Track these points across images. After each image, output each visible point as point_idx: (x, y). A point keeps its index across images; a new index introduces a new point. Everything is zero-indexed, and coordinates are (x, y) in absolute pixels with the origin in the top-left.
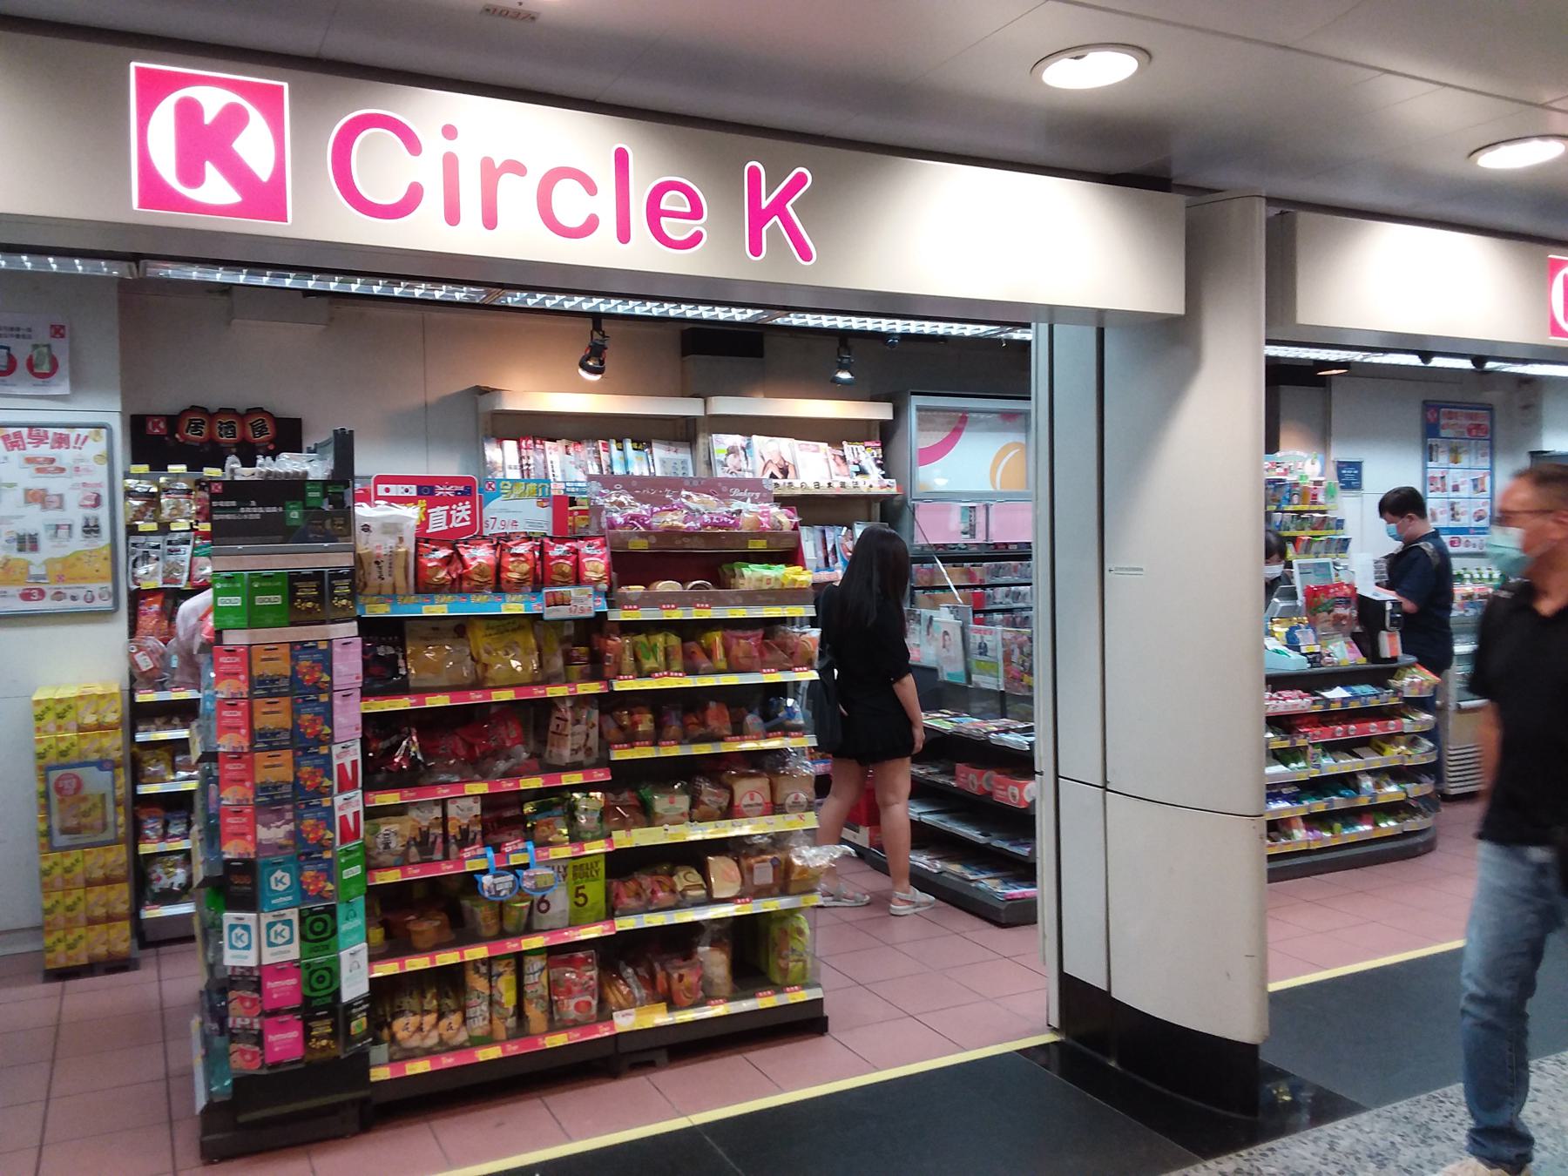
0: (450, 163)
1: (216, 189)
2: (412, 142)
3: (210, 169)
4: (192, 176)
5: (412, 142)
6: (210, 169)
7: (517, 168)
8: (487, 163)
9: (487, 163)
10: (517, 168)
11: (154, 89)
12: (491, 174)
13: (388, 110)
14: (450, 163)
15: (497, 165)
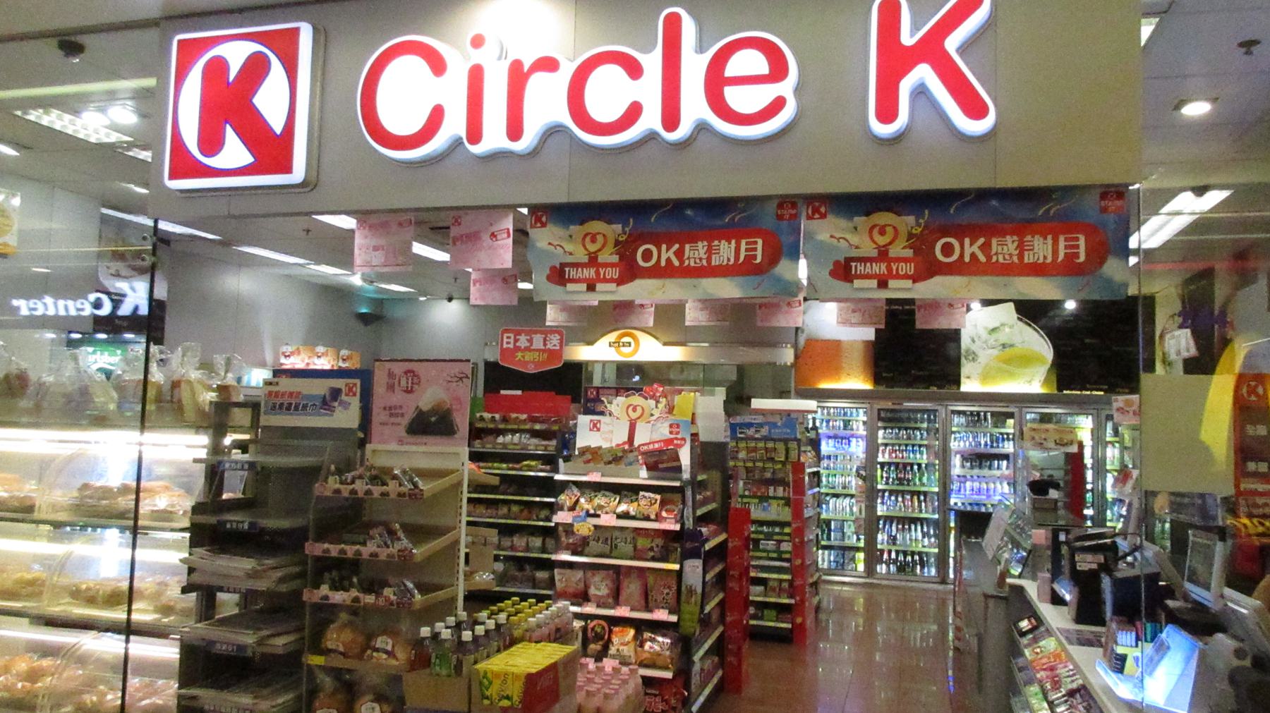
0: (476, 76)
1: (234, 152)
2: (437, 65)
3: (230, 135)
4: (211, 143)
5: (437, 65)
6: (230, 135)
7: (548, 64)
8: (516, 67)
9: (516, 67)
10: (548, 64)
11: (190, 51)
12: (518, 78)
13: (417, 34)
14: (476, 76)
15: (526, 68)
